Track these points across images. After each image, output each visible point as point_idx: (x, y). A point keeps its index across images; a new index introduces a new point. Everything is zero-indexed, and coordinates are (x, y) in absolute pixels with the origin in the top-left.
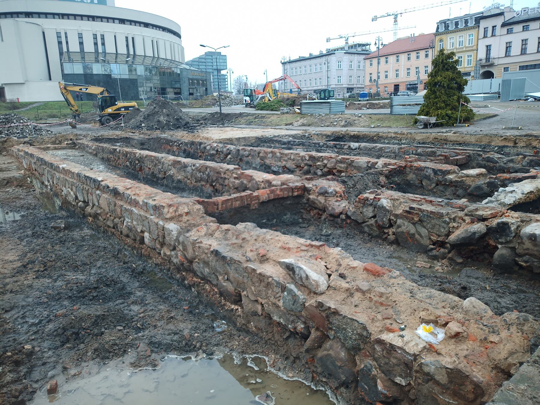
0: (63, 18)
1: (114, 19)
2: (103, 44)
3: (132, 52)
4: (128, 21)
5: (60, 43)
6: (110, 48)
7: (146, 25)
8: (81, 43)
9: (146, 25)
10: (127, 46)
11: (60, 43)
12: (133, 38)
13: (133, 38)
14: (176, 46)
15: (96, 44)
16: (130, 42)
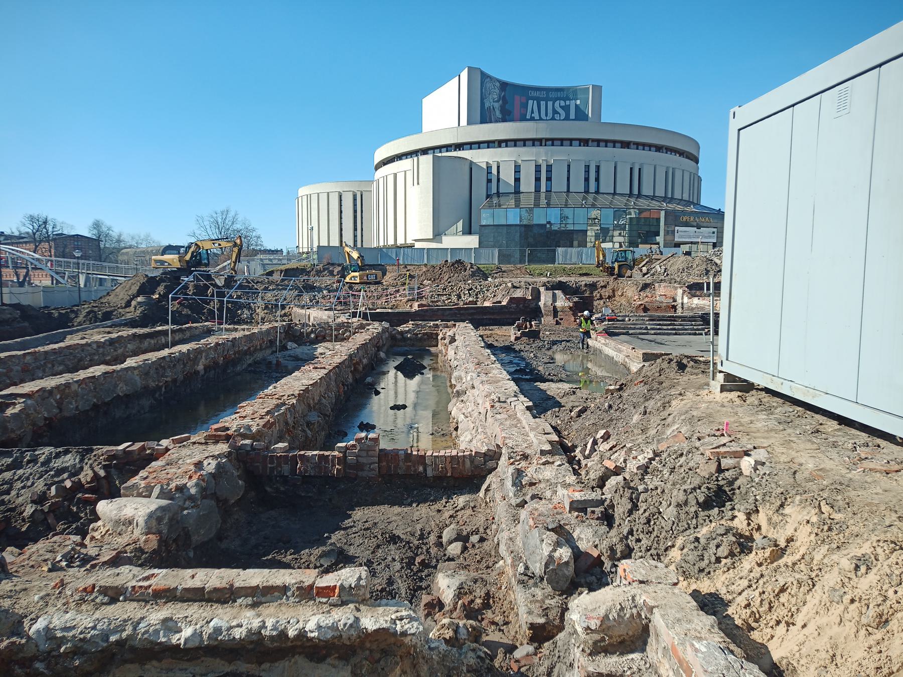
0: (500, 146)
1: (571, 141)
2: (549, 179)
3: (592, 188)
4: (593, 140)
5: (489, 181)
6: (559, 184)
7: (626, 145)
8: (517, 180)
9: (626, 145)
10: (587, 180)
11: (489, 181)
12: (598, 167)
13: (598, 167)
14: (678, 174)
15: (538, 179)
16: (592, 174)
